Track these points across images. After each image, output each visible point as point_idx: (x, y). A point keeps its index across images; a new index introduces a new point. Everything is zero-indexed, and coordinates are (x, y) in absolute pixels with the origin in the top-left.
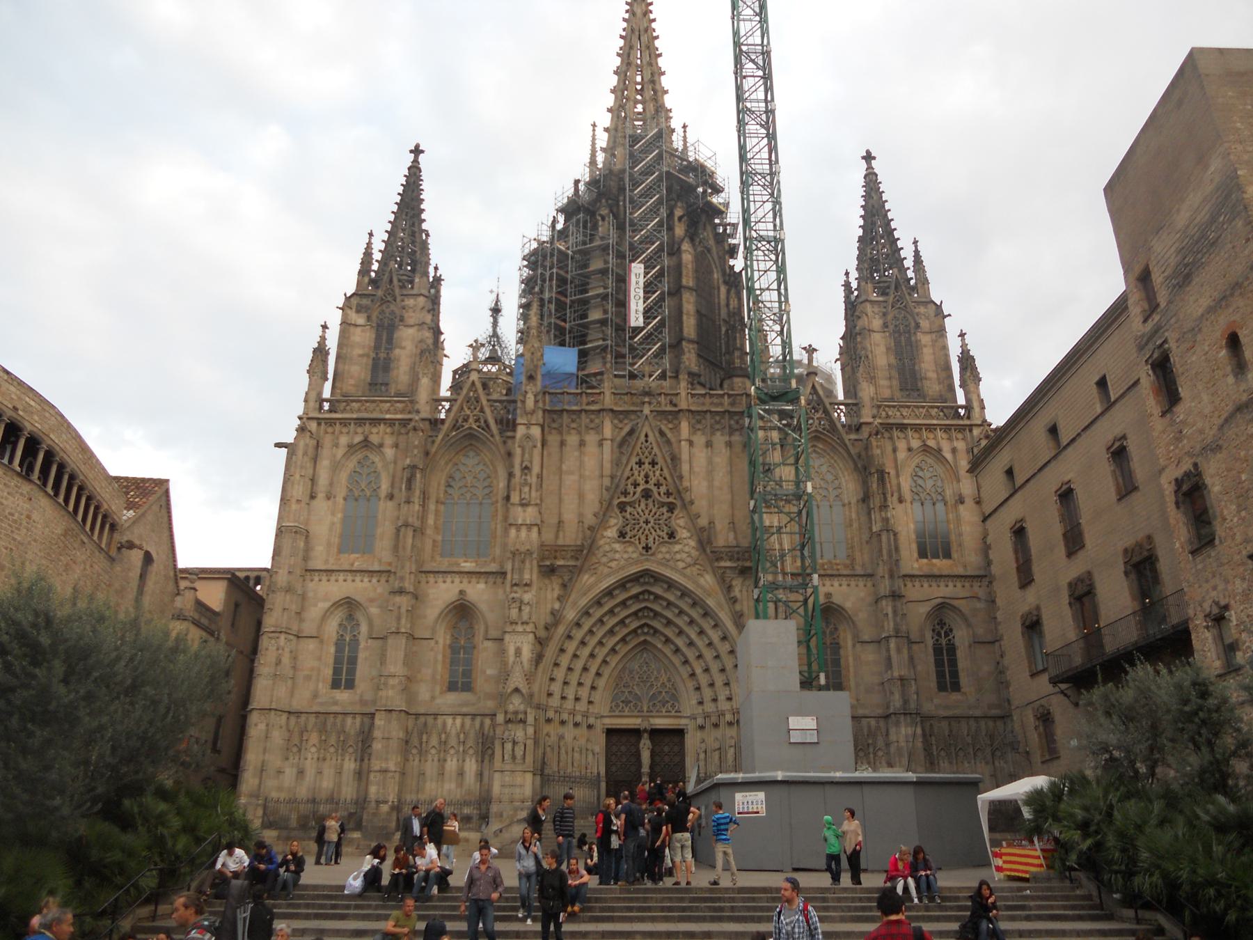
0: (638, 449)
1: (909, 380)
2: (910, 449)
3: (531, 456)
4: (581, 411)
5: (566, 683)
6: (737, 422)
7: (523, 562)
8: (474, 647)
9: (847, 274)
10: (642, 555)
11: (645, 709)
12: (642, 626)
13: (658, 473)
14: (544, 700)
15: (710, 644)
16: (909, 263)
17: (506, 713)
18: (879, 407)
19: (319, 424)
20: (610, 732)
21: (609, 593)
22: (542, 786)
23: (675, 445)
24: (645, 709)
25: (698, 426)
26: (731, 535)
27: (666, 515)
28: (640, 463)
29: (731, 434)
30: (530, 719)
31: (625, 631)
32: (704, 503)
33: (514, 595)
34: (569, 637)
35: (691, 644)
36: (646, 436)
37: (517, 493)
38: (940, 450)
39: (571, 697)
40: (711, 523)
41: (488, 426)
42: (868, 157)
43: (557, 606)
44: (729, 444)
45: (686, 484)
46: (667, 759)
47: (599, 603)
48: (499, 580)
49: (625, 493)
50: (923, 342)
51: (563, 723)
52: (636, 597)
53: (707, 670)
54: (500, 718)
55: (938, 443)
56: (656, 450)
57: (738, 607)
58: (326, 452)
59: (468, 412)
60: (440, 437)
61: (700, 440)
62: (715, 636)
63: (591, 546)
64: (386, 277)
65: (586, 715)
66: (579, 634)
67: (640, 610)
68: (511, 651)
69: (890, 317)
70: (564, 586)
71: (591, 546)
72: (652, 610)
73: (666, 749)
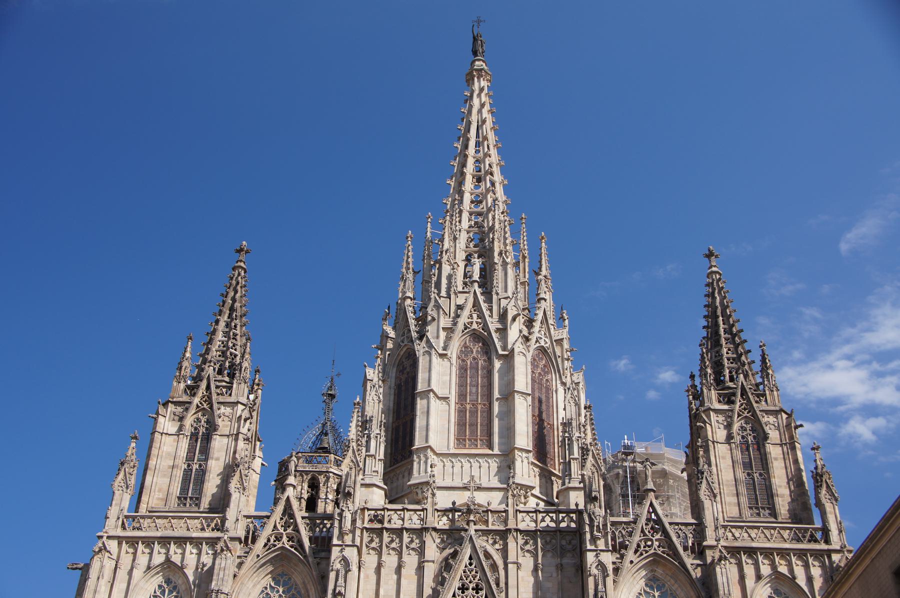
1: (761, 496)
2: (759, 577)
3: (345, 582)
6: (570, 542)
9: (692, 377)
16: (757, 367)
18: (725, 527)
19: (120, 544)
25: (528, 547)
29: (562, 556)
36: (470, 558)
38: (794, 578)
42: (710, 254)
44: (560, 567)
50: (773, 456)
55: (791, 570)
58: (122, 574)
59: (282, 531)
60: (249, 558)
61: (528, 562)
64: (204, 385)
69: (736, 427)
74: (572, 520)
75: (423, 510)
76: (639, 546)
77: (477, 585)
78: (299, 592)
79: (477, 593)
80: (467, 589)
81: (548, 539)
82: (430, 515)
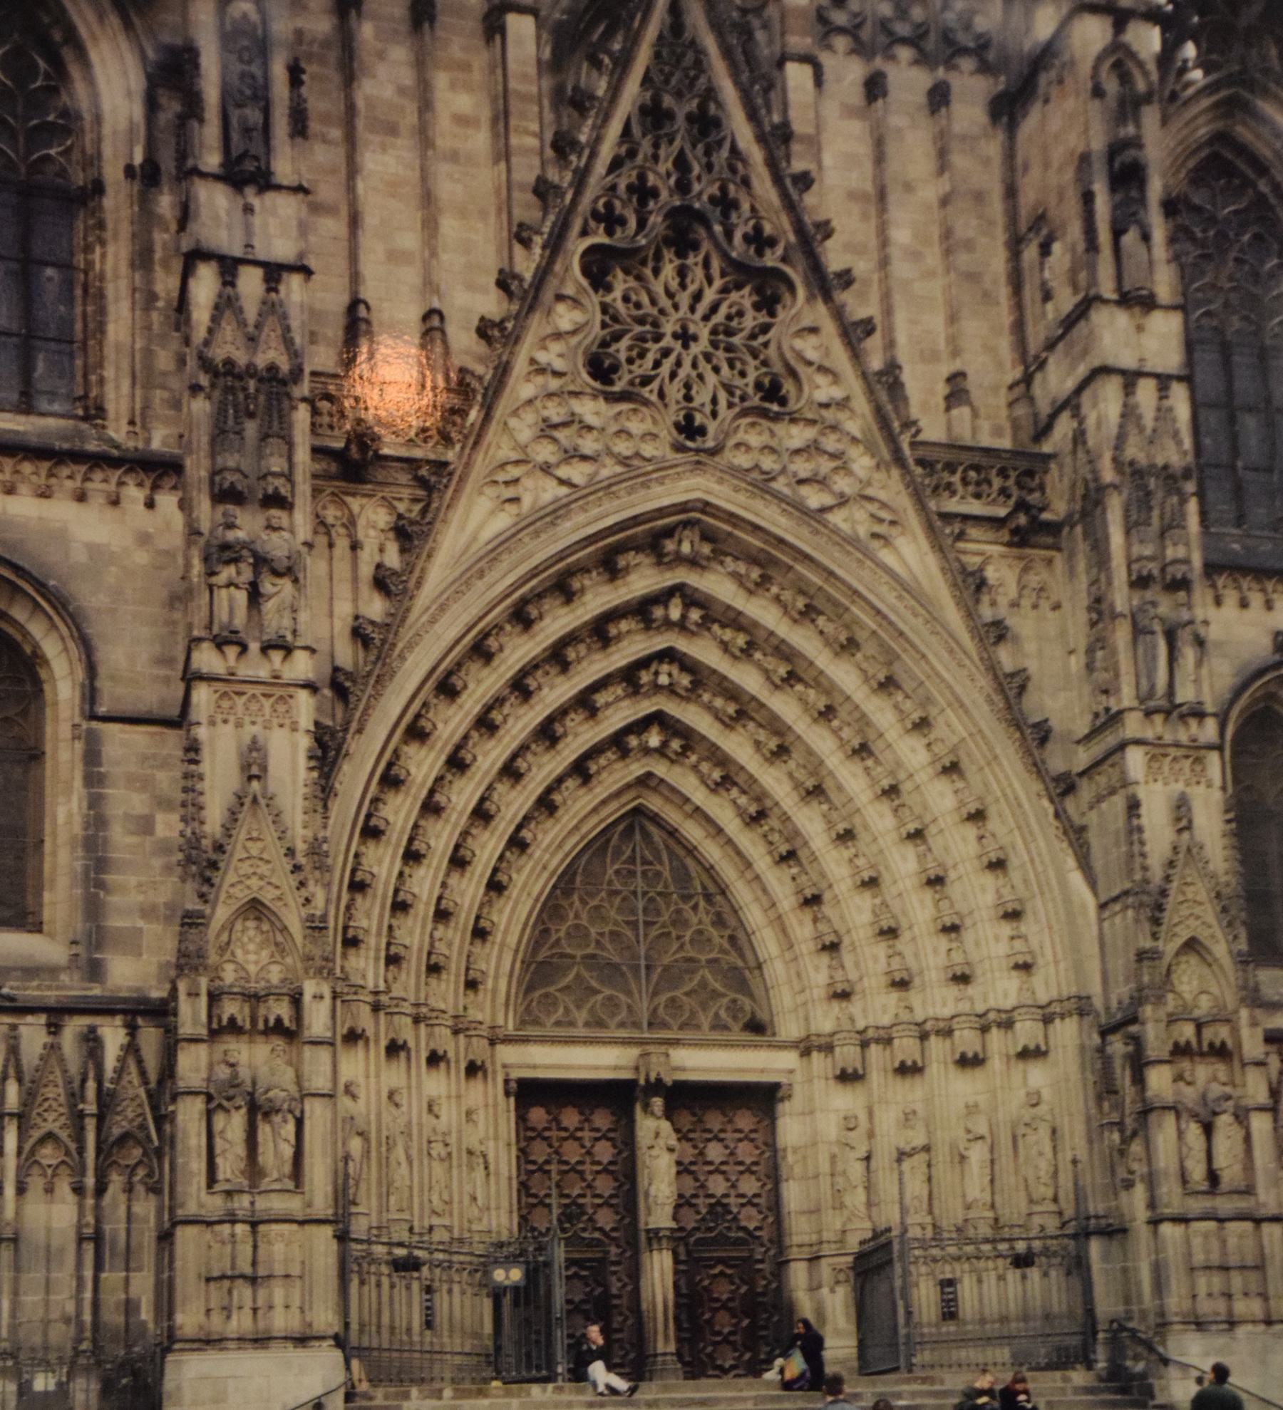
10: (679, 448)
30: (318, 1020)
43: (376, 607)
57: (1006, 658)
62: (912, 754)
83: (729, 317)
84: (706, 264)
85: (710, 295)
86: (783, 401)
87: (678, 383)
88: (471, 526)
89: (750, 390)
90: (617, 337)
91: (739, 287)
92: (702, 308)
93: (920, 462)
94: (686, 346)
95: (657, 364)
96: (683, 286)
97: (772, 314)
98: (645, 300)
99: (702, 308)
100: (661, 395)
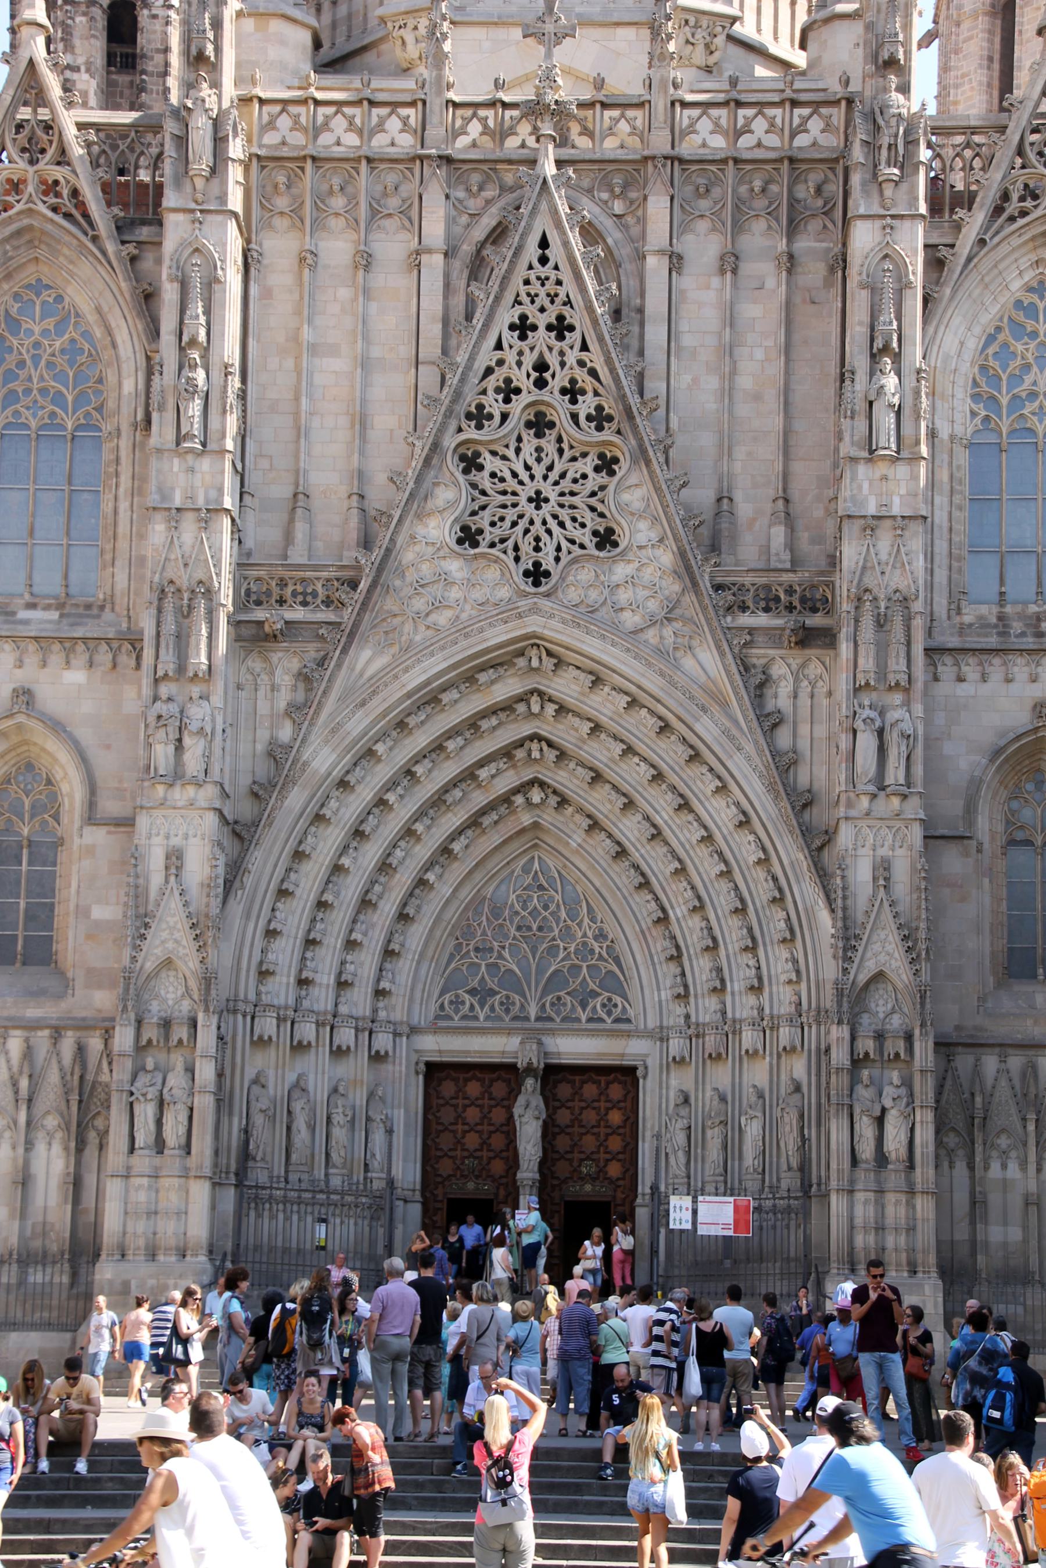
0: (516, 284)
4: (358, 160)
5: (310, 943)
7: (186, 613)
8: (60, 842)
10: (526, 595)
11: (533, 1011)
12: (523, 789)
13: (571, 358)
14: (248, 987)
15: (708, 839)
17: (139, 1022)
20: (435, 1072)
21: (430, 699)
22: (239, 1216)
23: (628, 267)
24: (533, 1011)
25: (704, 204)
26: (779, 534)
27: (595, 480)
28: (523, 328)
29: (793, 229)
31: (479, 799)
32: (707, 440)
33: (160, 707)
34: (319, 818)
35: (657, 836)
36: (544, 244)
37: (170, 415)
39: (326, 978)
40: (723, 498)
41: (81, 206)
45: (655, 386)
46: (589, 1142)
47: (401, 725)
48: (126, 660)
49: (479, 417)
51: (299, 1048)
52: (506, 708)
53: (699, 908)
54: (124, 1038)
56: (569, 287)
62: (720, 814)
63: (380, 570)
65: (368, 1028)
66: (348, 810)
67: (520, 744)
68: (156, 861)
70: (304, 678)
71: (380, 570)
72: (550, 744)
73: (590, 1117)
74: (827, 128)
75: (413, 104)
76: (1006, 196)
77: (561, 318)
78: (87, 335)
79: (561, 337)
80: (534, 328)
81: (757, 184)
82: (433, 119)
83: (575, 481)
84: (560, 440)
85: (558, 469)
86: (615, 544)
87: (530, 537)
88: (359, 666)
89: (588, 539)
90: (483, 508)
91: (584, 455)
92: (554, 476)
93: (718, 587)
94: (538, 508)
95: (514, 524)
96: (539, 460)
97: (612, 473)
98: (507, 475)
99: (554, 476)
100: (516, 548)
